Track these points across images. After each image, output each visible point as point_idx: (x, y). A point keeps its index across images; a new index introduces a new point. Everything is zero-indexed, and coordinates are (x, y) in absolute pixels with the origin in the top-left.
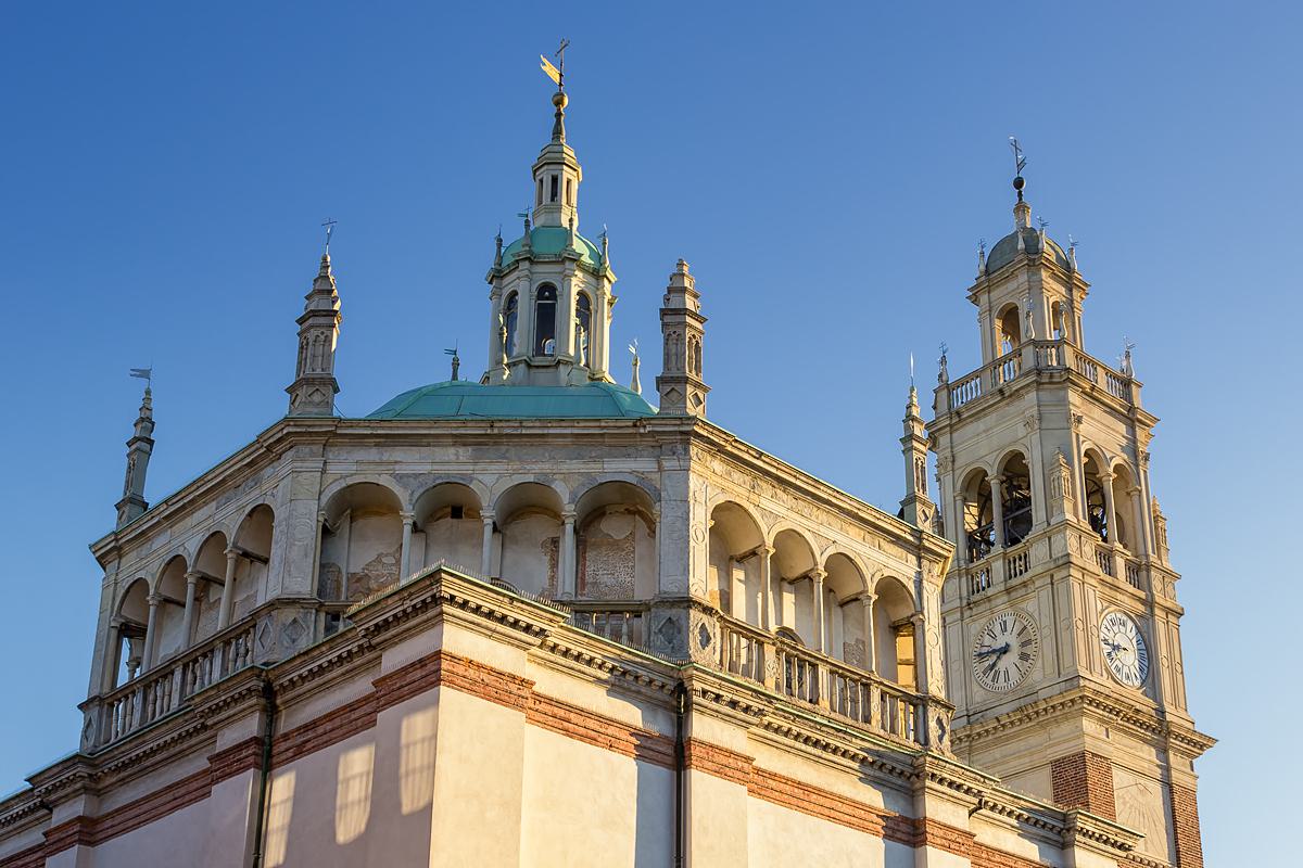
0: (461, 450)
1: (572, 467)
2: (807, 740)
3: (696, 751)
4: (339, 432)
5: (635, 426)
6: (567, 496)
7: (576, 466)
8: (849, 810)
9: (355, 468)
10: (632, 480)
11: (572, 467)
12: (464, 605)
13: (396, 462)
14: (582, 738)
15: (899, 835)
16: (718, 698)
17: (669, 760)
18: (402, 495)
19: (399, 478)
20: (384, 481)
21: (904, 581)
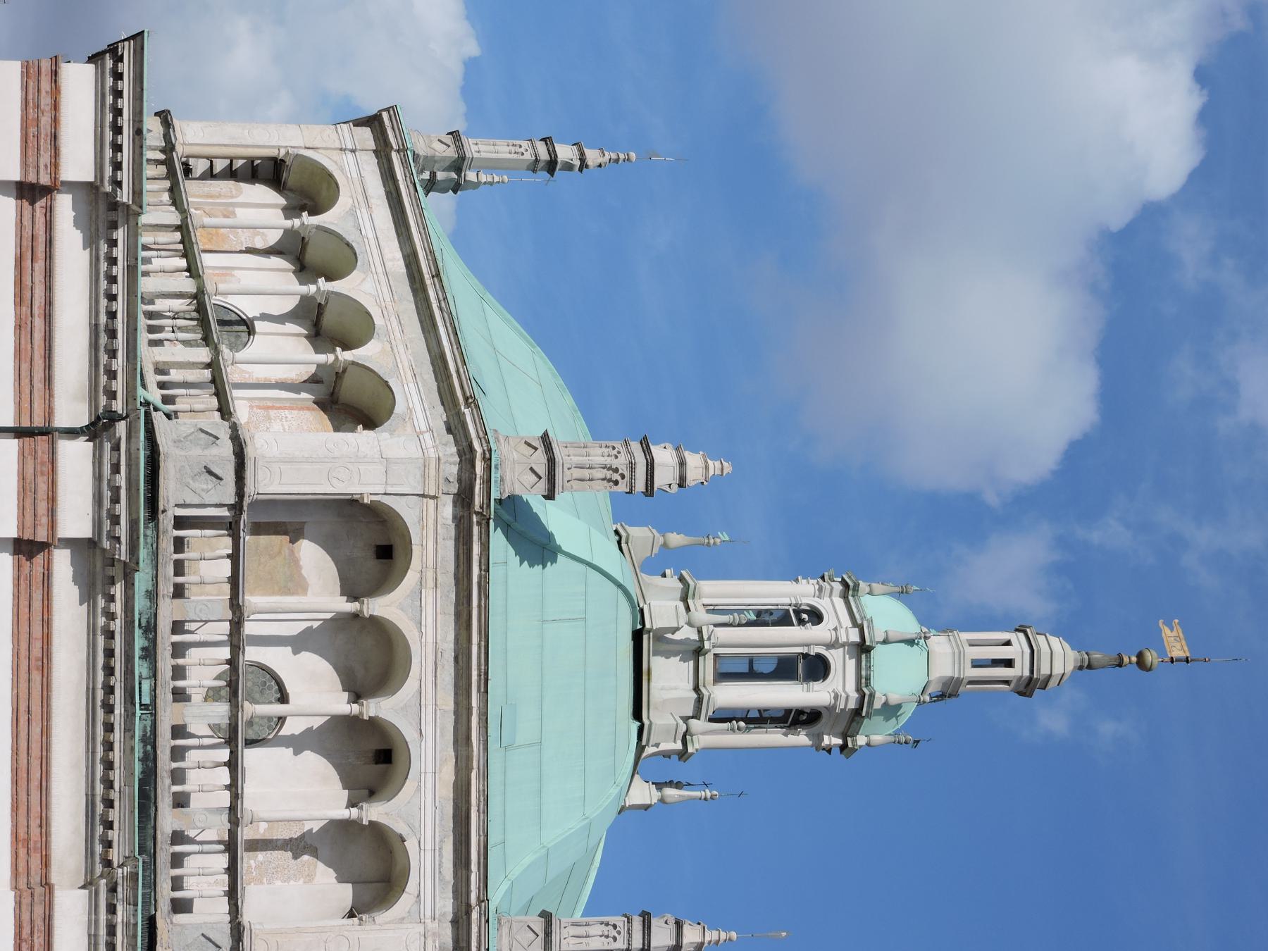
0: (401, 263)
1: (404, 357)
2: (109, 653)
3: (42, 441)
4: (394, 155)
5: (466, 399)
6: (366, 354)
7: (404, 359)
8: (35, 751)
9: (355, 175)
10: (399, 408)
11: (404, 357)
12: (118, 76)
14: (19, 282)
15: (22, 852)
16: (116, 469)
17: (26, 423)
20: (344, 201)
21: (411, 886)
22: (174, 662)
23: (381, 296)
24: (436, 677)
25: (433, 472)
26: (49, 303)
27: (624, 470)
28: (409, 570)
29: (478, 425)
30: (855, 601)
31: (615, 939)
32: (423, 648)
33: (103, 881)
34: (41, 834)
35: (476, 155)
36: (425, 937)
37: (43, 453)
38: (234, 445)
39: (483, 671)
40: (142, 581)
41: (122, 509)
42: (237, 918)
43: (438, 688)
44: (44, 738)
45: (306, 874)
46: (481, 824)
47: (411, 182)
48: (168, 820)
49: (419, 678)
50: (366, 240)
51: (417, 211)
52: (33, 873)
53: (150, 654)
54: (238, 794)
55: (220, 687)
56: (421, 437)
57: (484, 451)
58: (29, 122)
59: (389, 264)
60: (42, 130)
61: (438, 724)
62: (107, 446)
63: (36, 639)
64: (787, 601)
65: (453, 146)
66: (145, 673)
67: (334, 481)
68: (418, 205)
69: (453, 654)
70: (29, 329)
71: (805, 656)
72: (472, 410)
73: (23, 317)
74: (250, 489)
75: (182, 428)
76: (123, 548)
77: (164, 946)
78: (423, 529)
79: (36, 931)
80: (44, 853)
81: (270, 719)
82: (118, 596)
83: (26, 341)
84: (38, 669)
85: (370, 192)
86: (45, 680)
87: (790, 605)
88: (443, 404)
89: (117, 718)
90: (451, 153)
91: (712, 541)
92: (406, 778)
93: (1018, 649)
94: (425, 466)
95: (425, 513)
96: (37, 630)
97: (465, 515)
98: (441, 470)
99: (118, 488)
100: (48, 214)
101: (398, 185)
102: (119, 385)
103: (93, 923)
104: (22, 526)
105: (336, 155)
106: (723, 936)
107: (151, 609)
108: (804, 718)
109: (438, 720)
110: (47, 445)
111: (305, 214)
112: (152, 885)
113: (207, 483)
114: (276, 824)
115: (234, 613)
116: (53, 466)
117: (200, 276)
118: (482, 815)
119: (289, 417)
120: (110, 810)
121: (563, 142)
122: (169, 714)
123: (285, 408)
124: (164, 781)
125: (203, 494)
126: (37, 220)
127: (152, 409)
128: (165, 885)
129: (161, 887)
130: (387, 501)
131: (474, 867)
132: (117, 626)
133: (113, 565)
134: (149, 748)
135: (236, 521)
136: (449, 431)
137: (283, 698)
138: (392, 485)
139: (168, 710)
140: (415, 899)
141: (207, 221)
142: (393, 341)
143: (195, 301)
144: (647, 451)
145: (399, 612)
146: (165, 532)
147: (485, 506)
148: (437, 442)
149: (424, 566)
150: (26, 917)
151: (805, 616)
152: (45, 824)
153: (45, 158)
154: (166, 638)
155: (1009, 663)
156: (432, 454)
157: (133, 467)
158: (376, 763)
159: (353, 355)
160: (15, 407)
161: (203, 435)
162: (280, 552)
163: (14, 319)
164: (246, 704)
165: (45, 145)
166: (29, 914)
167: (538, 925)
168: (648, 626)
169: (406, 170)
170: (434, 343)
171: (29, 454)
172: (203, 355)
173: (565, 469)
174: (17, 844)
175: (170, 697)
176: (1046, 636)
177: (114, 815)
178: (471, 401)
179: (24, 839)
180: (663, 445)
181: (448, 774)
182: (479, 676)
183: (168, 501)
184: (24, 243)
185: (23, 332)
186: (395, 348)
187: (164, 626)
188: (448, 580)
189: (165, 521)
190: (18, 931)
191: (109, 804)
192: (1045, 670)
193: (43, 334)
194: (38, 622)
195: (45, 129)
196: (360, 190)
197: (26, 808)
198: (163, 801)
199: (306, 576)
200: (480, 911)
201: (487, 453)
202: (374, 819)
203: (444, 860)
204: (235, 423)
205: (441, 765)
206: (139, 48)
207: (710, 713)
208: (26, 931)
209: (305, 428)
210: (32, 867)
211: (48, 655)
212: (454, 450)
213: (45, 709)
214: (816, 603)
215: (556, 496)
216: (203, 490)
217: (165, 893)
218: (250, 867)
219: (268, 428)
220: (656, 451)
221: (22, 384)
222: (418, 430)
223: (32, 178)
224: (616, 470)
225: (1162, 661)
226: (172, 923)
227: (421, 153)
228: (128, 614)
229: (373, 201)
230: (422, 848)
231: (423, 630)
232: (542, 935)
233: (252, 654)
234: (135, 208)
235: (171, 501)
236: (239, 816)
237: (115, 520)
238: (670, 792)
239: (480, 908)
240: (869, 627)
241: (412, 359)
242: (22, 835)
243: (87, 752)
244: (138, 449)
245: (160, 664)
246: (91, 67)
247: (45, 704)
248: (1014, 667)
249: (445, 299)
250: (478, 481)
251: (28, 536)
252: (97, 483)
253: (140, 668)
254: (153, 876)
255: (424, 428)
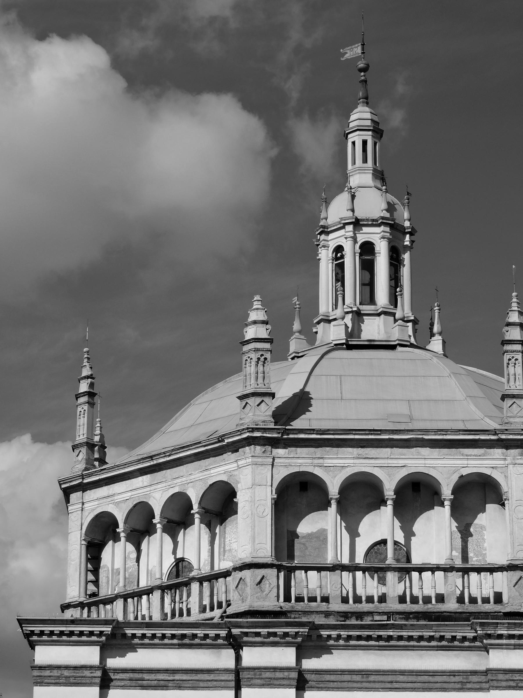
0: (145, 477)
2: (359, 638)
3: (243, 675)
4: (85, 481)
5: (219, 441)
6: (195, 496)
9: (96, 503)
10: (224, 478)
12: (42, 633)
13: (114, 495)
15: (469, 686)
16: (258, 634)
17: (233, 684)
18: (120, 518)
19: (117, 504)
20: (111, 509)
21: (488, 472)
22: (364, 603)
23: (163, 488)
24: (372, 458)
25: (260, 460)
26: (166, 671)
27: (258, 355)
28: (314, 473)
29: (234, 435)
30: (330, 227)
31: (516, 360)
32: (357, 465)
33: (485, 641)
34: (459, 675)
35: (85, 436)
36: (516, 464)
37: (249, 674)
38: (245, 569)
39: (369, 432)
40: (319, 620)
41: (280, 631)
42: (505, 567)
43: (378, 457)
44: (406, 674)
45: (480, 529)
46: (453, 433)
47: (100, 472)
48: (451, 606)
49: (373, 468)
50: (132, 497)
51: (116, 468)
52: (480, 680)
53: (360, 615)
54: (437, 567)
55: (378, 577)
56: (240, 466)
57: (248, 432)
58: (67, 682)
59: (146, 484)
60: (72, 675)
61: (398, 457)
62: (245, 639)
63: (351, 678)
64: (330, 265)
65: (80, 449)
66: (370, 618)
67: (265, 514)
68: (113, 468)
69: (360, 449)
70: (181, 682)
71: (361, 255)
72: (225, 438)
73: (175, 685)
74: (269, 560)
75: (235, 598)
76: (301, 630)
77: (520, 607)
78: (291, 465)
79: (511, 678)
80: (469, 674)
81: (395, 549)
82: (328, 633)
83: (188, 683)
84: (368, 677)
85: (106, 494)
86: (374, 673)
87: (333, 263)
88: (222, 454)
89: (395, 633)
90: (84, 450)
91: (298, 306)
92: (428, 474)
93: (356, 138)
94: (256, 464)
95: (282, 464)
96: (347, 677)
97: (283, 442)
98: (259, 455)
99: (268, 632)
100: (118, 671)
101: (102, 479)
102: (212, 633)
103: (508, 647)
104: (289, 686)
105: (85, 513)
106: (515, 300)
107: (335, 615)
108: (395, 255)
109: (396, 457)
110: (245, 672)
111: (118, 530)
112: (487, 615)
113: (266, 584)
114: (453, 546)
115: (338, 569)
116: (256, 669)
117: (151, 588)
118: (448, 433)
119: (229, 539)
120: (445, 637)
121: (78, 388)
122: (393, 606)
123: (224, 541)
124: (429, 608)
125: (272, 586)
126: (121, 678)
127: (225, 614)
128: (487, 607)
129: (488, 609)
130: (275, 485)
131: (477, 437)
132: (344, 633)
133: (311, 636)
134: (411, 616)
135: (287, 568)
136: (237, 451)
137: (384, 542)
138: (267, 482)
139: (390, 605)
140: (494, 470)
141: (121, 584)
142: (188, 482)
143: (166, 591)
144: (248, 342)
145: (336, 478)
146: (293, 607)
147: (278, 431)
148: (243, 457)
149: (311, 464)
150: (504, 684)
151: (339, 255)
152: (453, 673)
153: (87, 673)
154: (351, 607)
155: (365, 143)
156: (249, 460)
157: (257, 625)
158: (419, 490)
159: (195, 504)
160: (224, 690)
161: (239, 586)
162: (304, 544)
163: (176, 690)
164: (387, 562)
165: (79, 673)
166: (503, 683)
167: (509, 402)
168: (344, 341)
169: (93, 474)
170: (189, 459)
171: (250, 681)
172: (195, 586)
173: (258, 387)
174: (464, 689)
175: (383, 605)
176: (350, 122)
177: (448, 635)
178: (221, 439)
179: (462, 685)
180: (245, 333)
181: (425, 451)
182: (371, 434)
183: (275, 605)
184: (134, 684)
185: (183, 685)
186: (191, 481)
187: (344, 608)
188: (319, 452)
189: (287, 607)
190: (512, 688)
191: (442, 638)
192: (369, 123)
193: (184, 674)
194: (342, 677)
195: (71, 673)
196: (105, 500)
197: (444, 684)
198: (440, 608)
199: (317, 530)
200: (501, 434)
201: (249, 430)
202: (450, 492)
203: (473, 454)
204: (232, 569)
205: (421, 455)
206: (26, 622)
207: (392, 307)
208: (512, 684)
209: (235, 530)
210: (477, 680)
211: (360, 672)
212: (247, 448)
213: (390, 673)
214: (331, 249)
215: (273, 392)
216: (269, 586)
217: (491, 607)
218: (477, 560)
219: (236, 551)
220: (248, 337)
221: (211, 686)
222: (236, 468)
223: (98, 681)
224: (259, 359)
225: (364, 58)
226: (508, 603)
227: (84, 466)
228: (338, 627)
229: (111, 493)
230: (466, 466)
231: (347, 465)
232: (514, 400)
233: (359, 559)
234: (114, 624)
235: (275, 604)
236: (449, 566)
237: (286, 634)
238: (436, 329)
239: (499, 434)
240: (345, 220)
241: (197, 471)
242: (459, 686)
243: (413, 650)
244: (247, 622)
245: (365, 610)
246: (37, 648)
247: (387, 673)
248: (367, 140)
249: (164, 453)
250: (265, 435)
251: (295, 683)
252: (266, 645)
253: (367, 621)
254: (482, 614)
255: (235, 465)
